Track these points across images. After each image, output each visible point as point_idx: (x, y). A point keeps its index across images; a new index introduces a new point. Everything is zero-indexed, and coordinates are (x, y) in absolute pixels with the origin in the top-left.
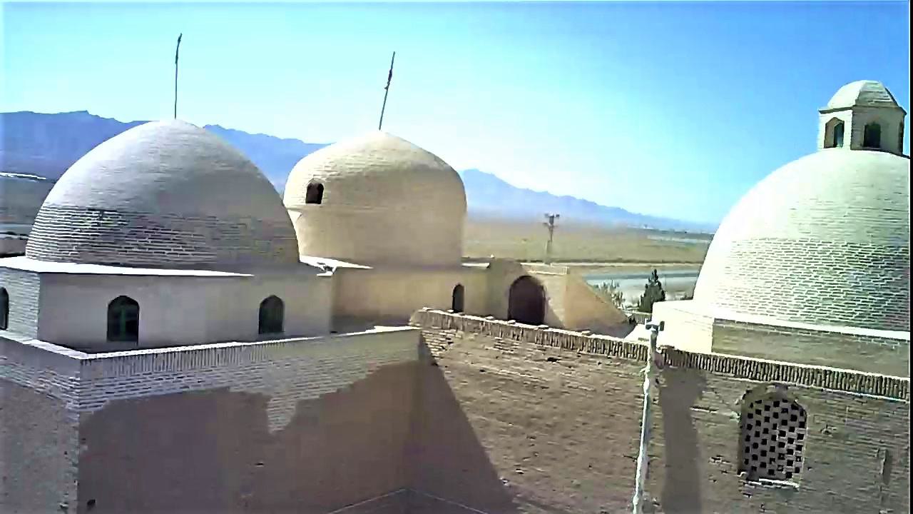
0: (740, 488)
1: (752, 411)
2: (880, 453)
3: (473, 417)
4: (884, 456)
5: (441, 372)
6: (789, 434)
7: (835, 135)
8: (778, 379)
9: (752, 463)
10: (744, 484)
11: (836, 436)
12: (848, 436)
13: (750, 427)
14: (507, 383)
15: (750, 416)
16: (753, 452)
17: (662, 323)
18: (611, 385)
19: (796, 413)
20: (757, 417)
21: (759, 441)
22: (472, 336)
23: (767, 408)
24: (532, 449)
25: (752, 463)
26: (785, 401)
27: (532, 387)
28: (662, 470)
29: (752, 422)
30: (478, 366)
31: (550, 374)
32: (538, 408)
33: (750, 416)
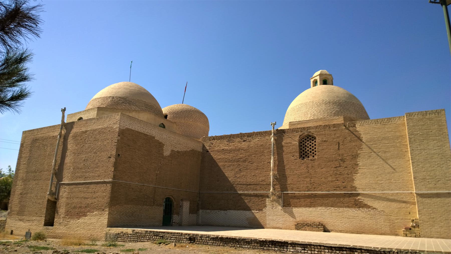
1: (302, 141)
3: (220, 164)
5: (210, 153)
6: (312, 145)
7: (315, 83)
9: (303, 156)
11: (325, 141)
13: (301, 146)
14: (230, 151)
15: (301, 143)
16: (303, 153)
18: (262, 143)
19: (313, 139)
20: (303, 143)
21: (304, 152)
22: (219, 141)
23: (306, 140)
24: (239, 169)
25: (303, 156)
26: (310, 136)
27: (239, 150)
28: (277, 162)
29: (302, 144)
30: (222, 148)
31: (244, 145)
32: (241, 156)
33: (301, 143)
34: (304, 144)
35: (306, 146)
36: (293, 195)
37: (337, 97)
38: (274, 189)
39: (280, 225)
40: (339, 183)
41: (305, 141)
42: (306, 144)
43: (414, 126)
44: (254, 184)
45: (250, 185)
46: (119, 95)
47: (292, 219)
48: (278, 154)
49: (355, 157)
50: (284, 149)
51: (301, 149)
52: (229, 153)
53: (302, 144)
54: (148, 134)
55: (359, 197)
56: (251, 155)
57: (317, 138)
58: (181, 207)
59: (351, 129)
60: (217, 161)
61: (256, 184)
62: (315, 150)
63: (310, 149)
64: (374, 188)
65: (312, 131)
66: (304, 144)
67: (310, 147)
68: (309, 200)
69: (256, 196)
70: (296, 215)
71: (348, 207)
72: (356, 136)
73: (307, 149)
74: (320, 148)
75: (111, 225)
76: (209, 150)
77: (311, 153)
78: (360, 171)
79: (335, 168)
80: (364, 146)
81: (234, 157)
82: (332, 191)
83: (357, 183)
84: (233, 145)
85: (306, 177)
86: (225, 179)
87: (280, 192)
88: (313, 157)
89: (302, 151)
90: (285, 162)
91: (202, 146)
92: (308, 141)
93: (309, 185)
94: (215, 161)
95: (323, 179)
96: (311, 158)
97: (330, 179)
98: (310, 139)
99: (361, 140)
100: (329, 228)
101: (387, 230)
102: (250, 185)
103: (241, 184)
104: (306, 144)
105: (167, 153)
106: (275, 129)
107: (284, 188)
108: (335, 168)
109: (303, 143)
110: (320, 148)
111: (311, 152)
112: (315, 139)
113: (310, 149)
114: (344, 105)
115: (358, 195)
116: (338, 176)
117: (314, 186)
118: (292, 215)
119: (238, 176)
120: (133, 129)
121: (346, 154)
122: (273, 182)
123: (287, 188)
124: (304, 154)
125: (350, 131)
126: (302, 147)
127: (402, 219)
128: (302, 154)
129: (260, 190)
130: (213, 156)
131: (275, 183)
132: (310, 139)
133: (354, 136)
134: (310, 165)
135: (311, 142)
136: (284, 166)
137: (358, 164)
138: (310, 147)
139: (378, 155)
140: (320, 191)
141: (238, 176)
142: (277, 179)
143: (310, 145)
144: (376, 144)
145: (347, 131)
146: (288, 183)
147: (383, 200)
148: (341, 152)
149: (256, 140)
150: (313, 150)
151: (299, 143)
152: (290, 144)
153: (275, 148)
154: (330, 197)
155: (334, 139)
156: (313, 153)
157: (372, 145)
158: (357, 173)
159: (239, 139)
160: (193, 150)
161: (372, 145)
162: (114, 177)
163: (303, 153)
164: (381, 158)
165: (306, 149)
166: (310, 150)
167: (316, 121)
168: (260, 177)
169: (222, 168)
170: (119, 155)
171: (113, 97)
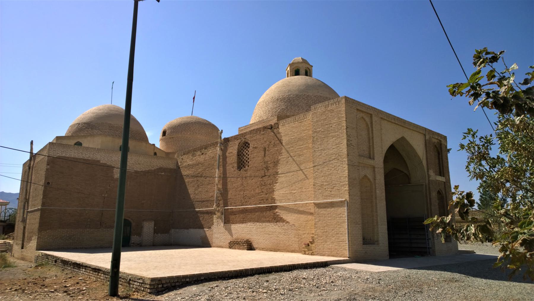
3: (186, 181)
31: (201, 159)
32: (199, 170)
37: (289, 91)
38: (218, 205)
39: (221, 244)
43: (317, 121)
46: (85, 121)
47: (230, 236)
48: (223, 166)
49: (276, 163)
52: (192, 168)
55: (277, 210)
58: (142, 227)
64: (289, 199)
68: (242, 215)
70: (233, 232)
71: (269, 221)
72: (278, 139)
73: (245, 158)
75: (38, 249)
76: (180, 167)
78: (280, 180)
80: (284, 151)
83: (277, 194)
85: (241, 190)
86: (188, 195)
97: (257, 191)
99: (282, 143)
100: (255, 245)
101: (296, 246)
102: (204, 201)
115: (276, 207)
118: (230, 231)
119: (197, 192)
120: (67, 156)
123: (227, 203)
126: (240, 157)
127: (308, 234)
133: (277, 139)
137: (278, 172)
139: (294, 160)
140: (250, 205)
144: (293, 147)
147: (295, 213)
151: (238, 152)
153: (221, 160)
154: (256, 212)
157: (290, 148)
158: (276, 183)
161: (290, 148)
162: (43, 204)
164: (296, 163)
167: (257, 125)
169: (187, 184)
170: (48, 183)
171: (79, 124)
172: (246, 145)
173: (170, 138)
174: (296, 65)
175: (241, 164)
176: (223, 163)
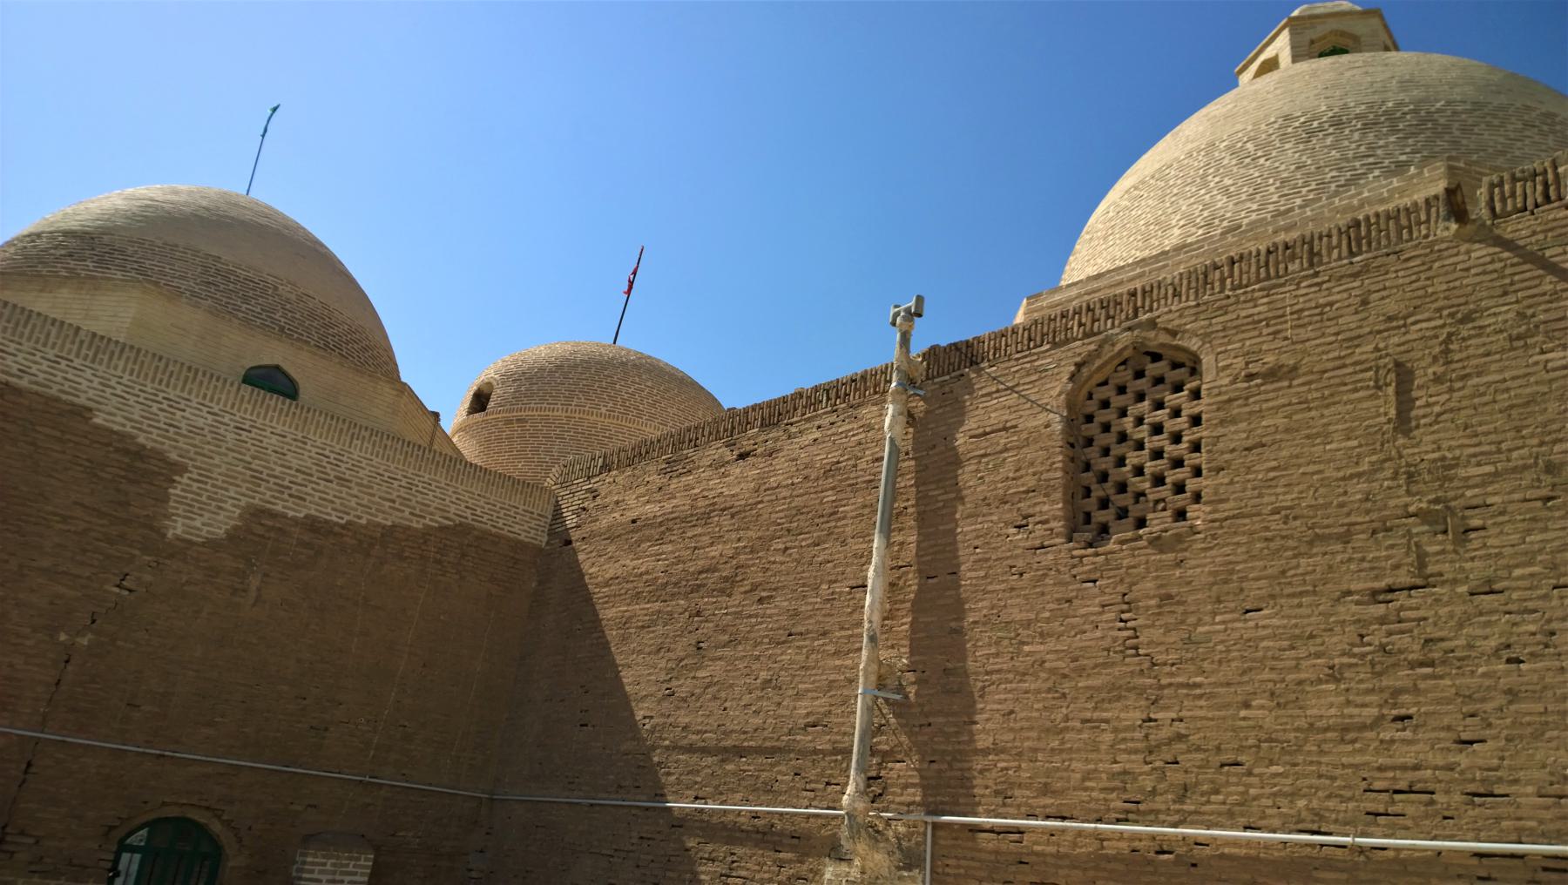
0: (1074, 572)
1: (1092, 407)
2: (1382, 372)
3: (608, 614)
4: (1392, 376)
6: (1171, 425)
8: (1136, 315)
9: (1100, 516)
10: (1082, 557)
11: (1272, 374)
12: (1295, 368)
13: (1089, 442)
14: (663, 528)
16: (1098, 492)
17: (920, 300)
20: (1102, 416)
22: (629, 472)
23: (1122, 390)
24: (693, 639)
25: (1100, 516)
26: (1156, 357)
27: (706, 517)
28: (912, 582)
29: (1093, 429)
30: (631, 515)
31: (738, 481)
32: (714, 552)
33: (1089, 419)
34: (1106, 428)
35: (1123, 437)
36: (1007, 844)
38: (875, 789)
40: (1417, 750)
41: (1117, 401)
42: (1128, 423)
44: (759, 751)
45: (740, 752)
48: (921, 518)
50: (966, 475)
51: (1087, 467)
52: (660, 540)
53: (1093, 429)
54: (24, 383)
56: (765, 542)
57: (1207, 361)
59: (1518, 228)
60: (599, 594)
61: (772, 752)
62: (1192, 459)
63: (1157, 454)
65: (1167, 312)
66: (1106, 428)
67: (1152, 442)
69: (766, 836)
73: (1133, 459)
74: (1236, 435)
76: (575, 535)
77: (1165, 491)
79: (1374, 596)
81: (679, 561)
82: (1346, 825)
84: (688, 488)
85: (1116, 692)
87: (918, 816)
88: (1181, 515)
89: (1089, 478)
90: (969, 575)
91: (551, 508)
92: (1140, 397)
93: (1134, 763)
94: (588, 599)
95: (1261, 712)
96: (1159, 522)
97: (1325, 705)
98: (1159, 380)
102: (740, 752)
103: (691, 749)
104: (1128, 423)
105: (200, 515)
106: (918, 346)
107: (947, 786)
108: (1374, 596)
109: (1102, 416)
110: (1236, 435)
111: (1159, 480)
112: (1195, 371)
113: (1157, 454)
114: (1466, 130)
116: (1402, 677)
117: (1175, 776)
119: (683, 687)
121: (1478, 459)
122: (873, 731)
123: (965, 782)
124: (1104, 504)
125: (1508, 245)
128: (1091, 504)
129: (790, 797)
130: (585, 567)
131: (884, 742)
132: (1159, 380)
134: (1149, 585)
135: (1159, 405)
136: (958, 608)
138: (1152, 442)
140: (1229, 818)
141: (683, 687)
142: (901, 709)
143: (1157, 429)
145: (1481, 252)
146: (983, 742)
148: (1423, 447)
149: (806, 444)
150: (1178, 463)
151: (1069, 422)
152: (1002, 439)
153: (907, 481)
155: (1355, 341)
156: (1180, 488)
159: (718, 451)
160: (461, 530)
163: (1098, 492)
165: (1121, 462)
166: (1150, 467)
168: (799, 696)
169: (612, 634)
171: (39, 235)
172: (1160, 367)
173: (508, 422)
174: (1333, 25)
175: (1101, 493)
176: (922, 499)
